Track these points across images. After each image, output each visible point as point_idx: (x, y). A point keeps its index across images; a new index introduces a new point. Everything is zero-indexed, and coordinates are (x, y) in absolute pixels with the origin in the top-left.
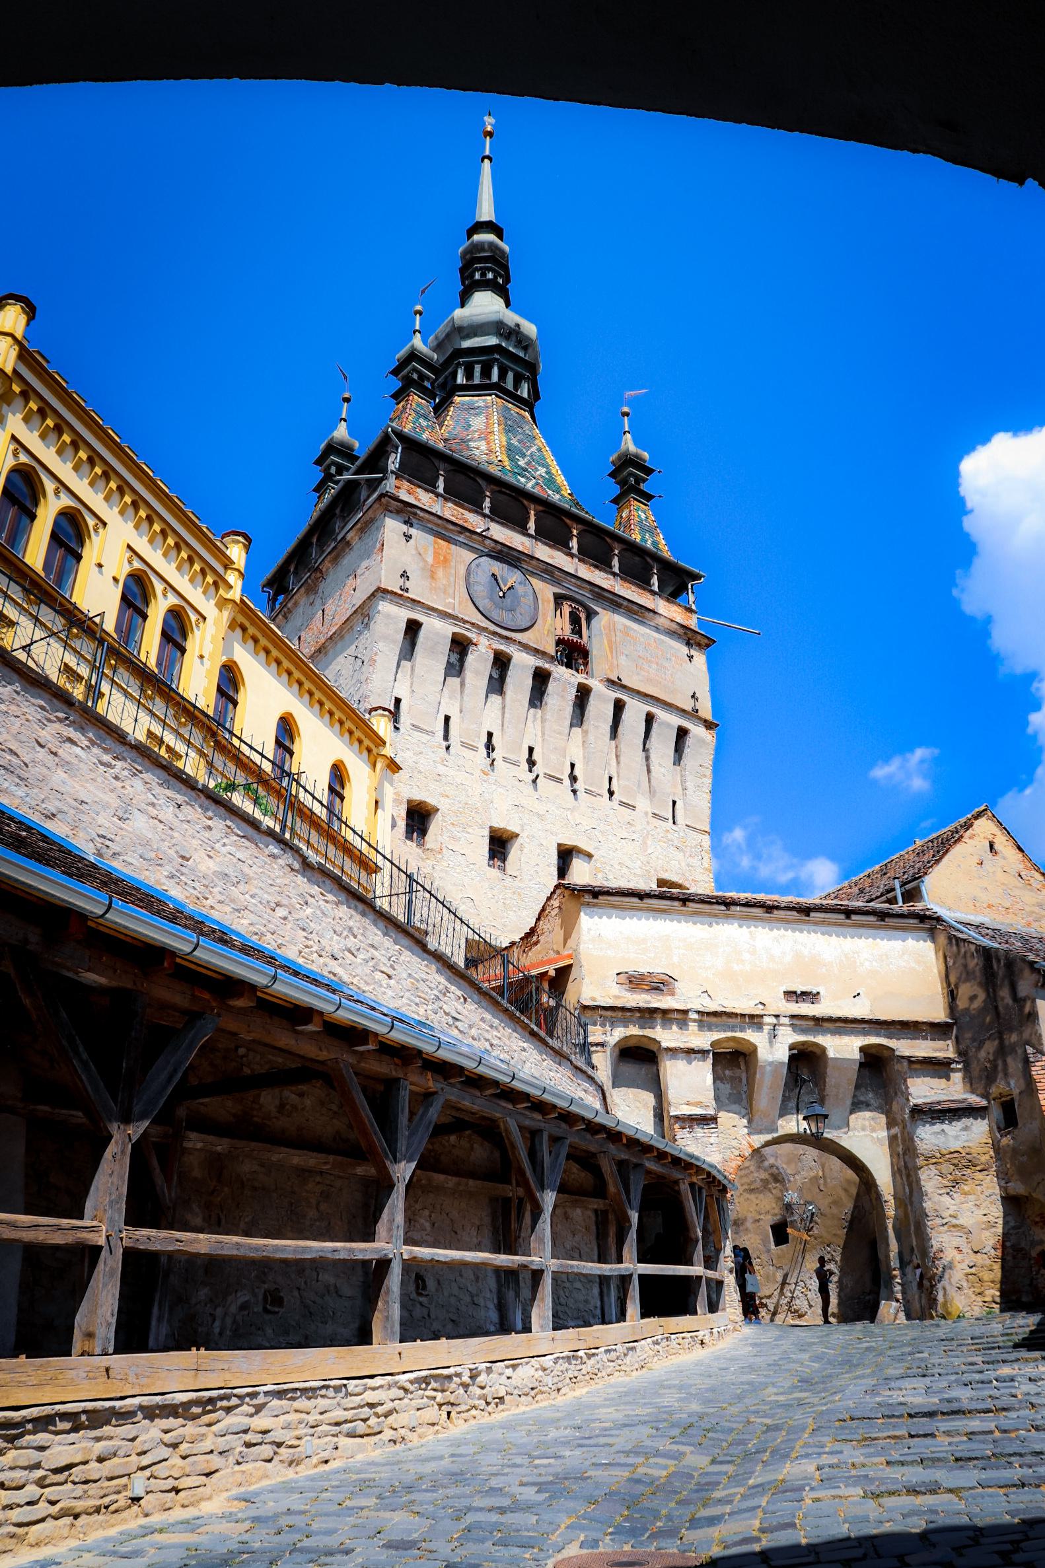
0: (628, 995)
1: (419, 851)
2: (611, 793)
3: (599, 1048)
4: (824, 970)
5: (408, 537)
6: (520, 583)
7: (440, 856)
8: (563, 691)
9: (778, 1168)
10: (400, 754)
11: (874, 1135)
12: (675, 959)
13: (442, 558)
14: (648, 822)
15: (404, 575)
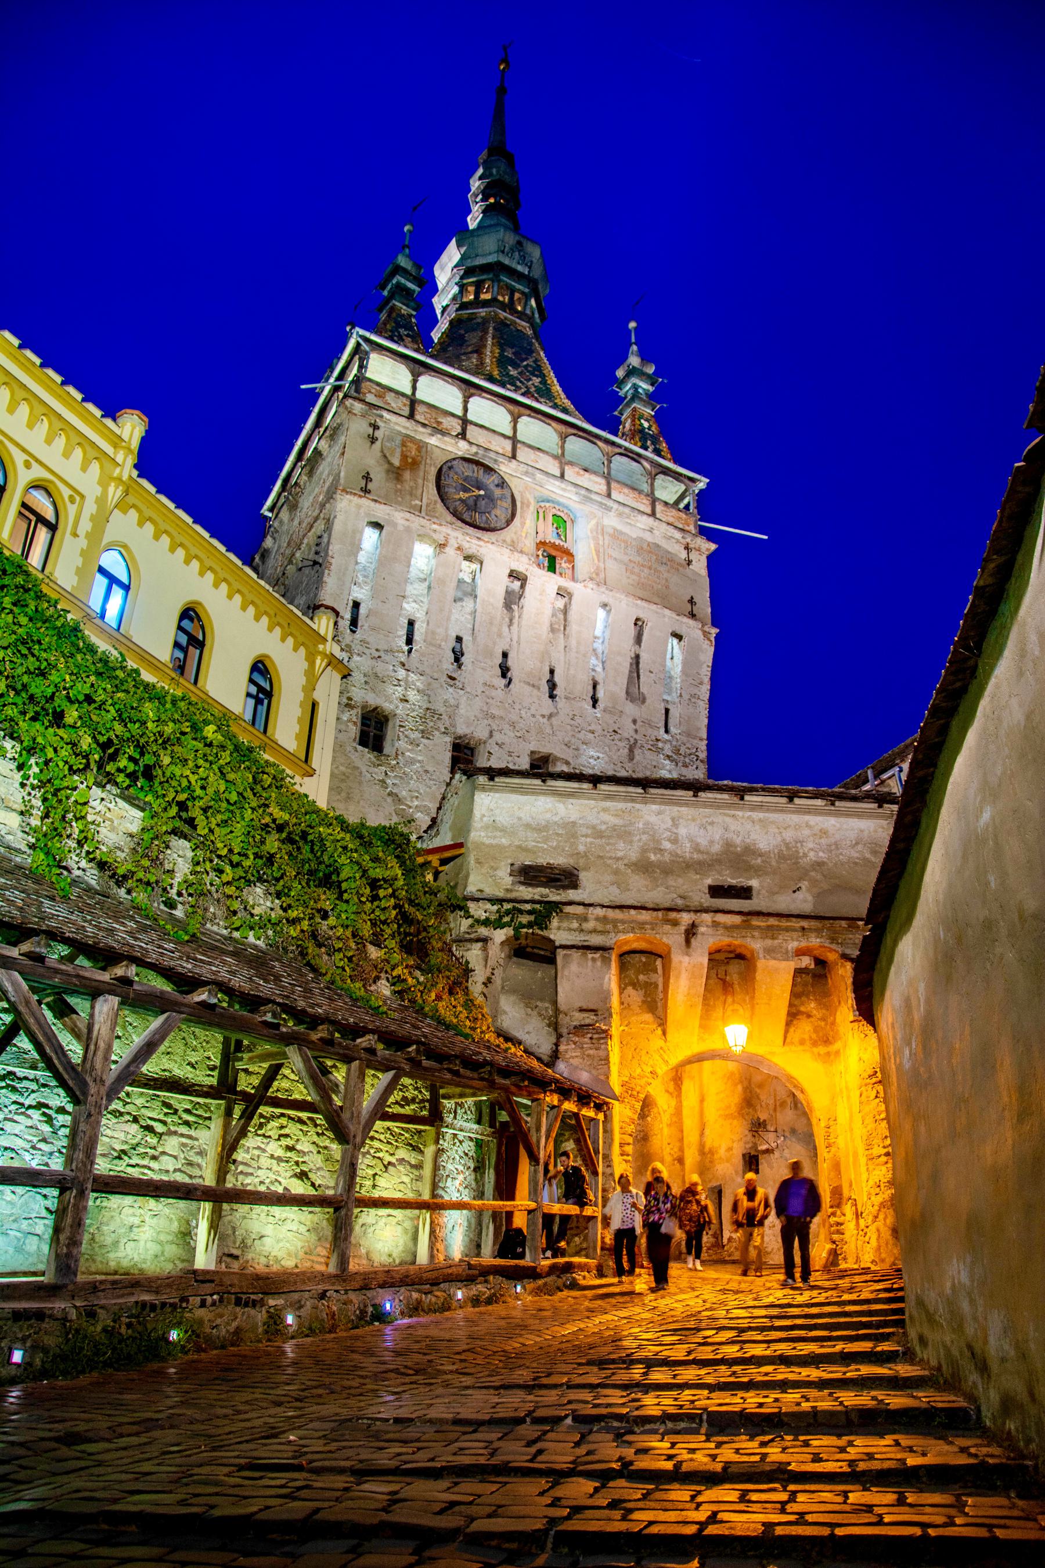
0: (522, 888)
1: (374, 759)
2: (595, 701)
3: (480, 945)
4: (759, 861)
5: (373, 440)
6: (497, 486)
7: (395, 762)
8: (541, 594)
9: (751, 1092)
10: (356, 658)
11: (815, 1050)
12: (581, 848)
13: (410, 460)
14: (636, 731)
15: (367, 478)
